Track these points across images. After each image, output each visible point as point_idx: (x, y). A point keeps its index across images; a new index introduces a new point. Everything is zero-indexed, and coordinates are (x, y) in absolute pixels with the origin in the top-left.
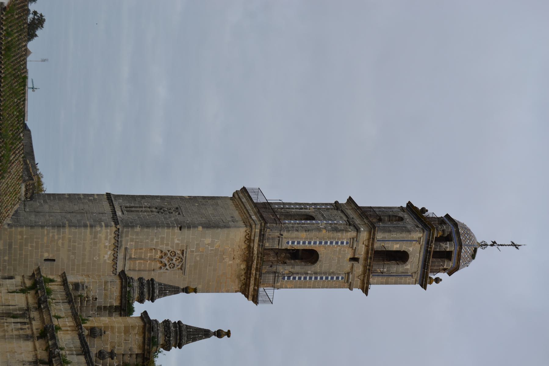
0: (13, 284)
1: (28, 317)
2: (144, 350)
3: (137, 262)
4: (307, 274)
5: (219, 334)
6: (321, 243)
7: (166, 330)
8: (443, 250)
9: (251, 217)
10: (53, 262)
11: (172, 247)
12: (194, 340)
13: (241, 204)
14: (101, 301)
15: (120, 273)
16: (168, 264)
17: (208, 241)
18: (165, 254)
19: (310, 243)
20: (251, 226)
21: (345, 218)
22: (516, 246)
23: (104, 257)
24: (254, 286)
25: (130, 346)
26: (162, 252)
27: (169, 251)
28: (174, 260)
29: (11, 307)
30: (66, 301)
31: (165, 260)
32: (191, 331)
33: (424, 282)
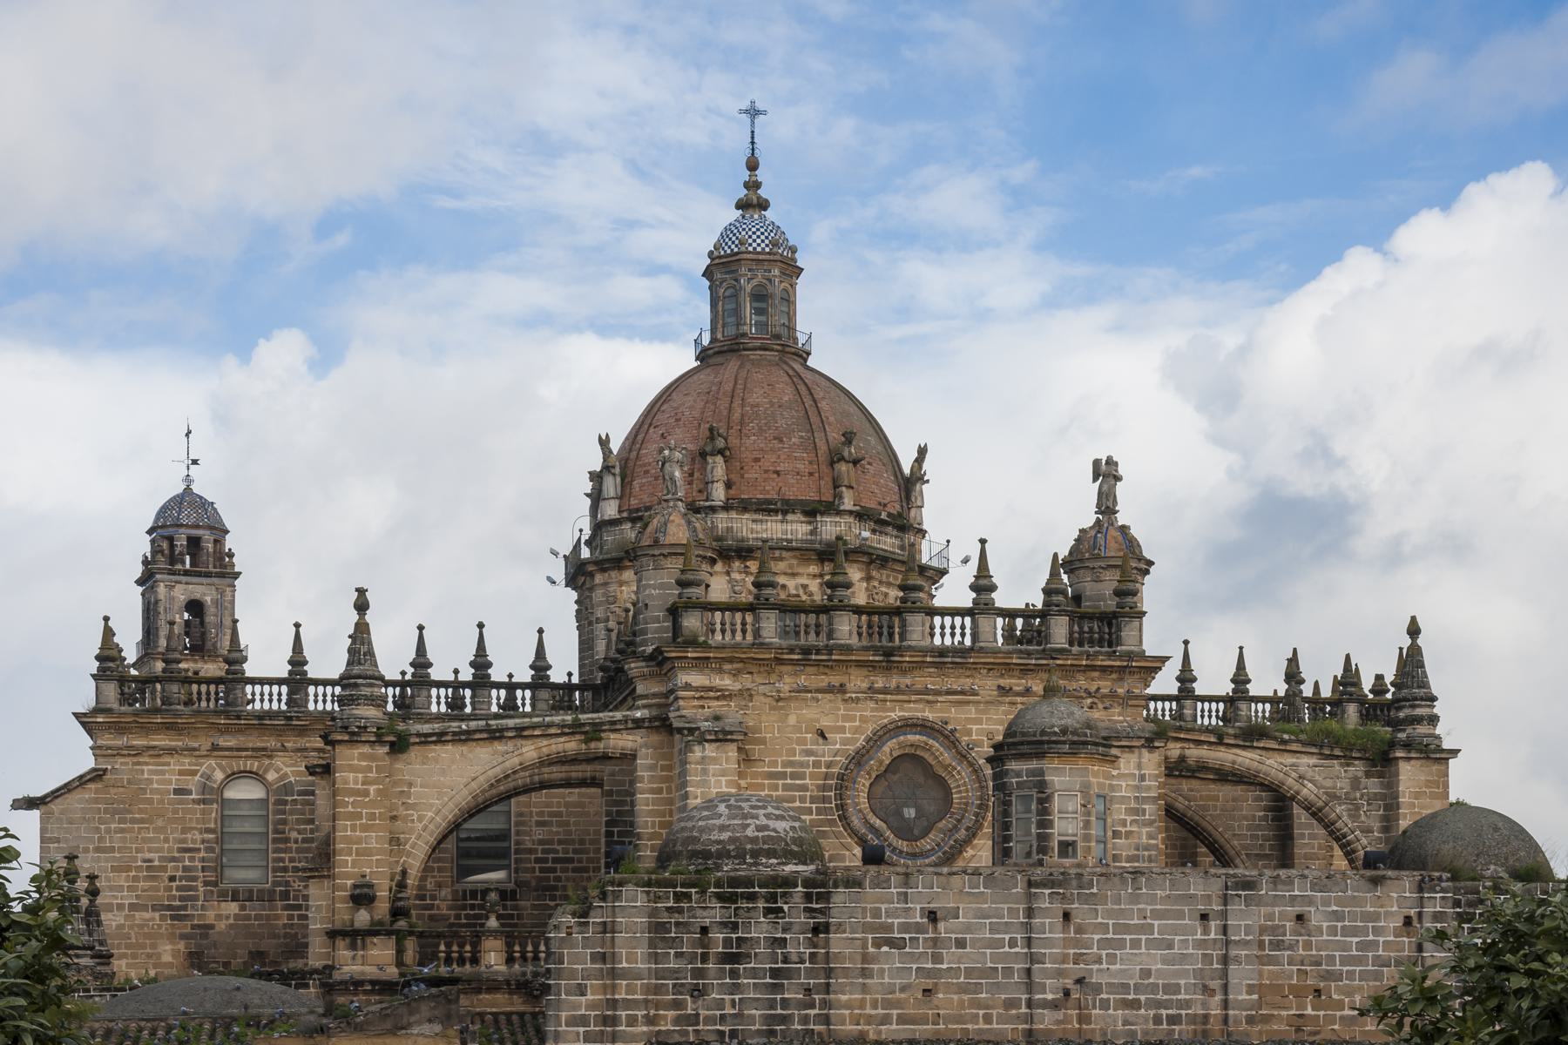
22: (188, 433)
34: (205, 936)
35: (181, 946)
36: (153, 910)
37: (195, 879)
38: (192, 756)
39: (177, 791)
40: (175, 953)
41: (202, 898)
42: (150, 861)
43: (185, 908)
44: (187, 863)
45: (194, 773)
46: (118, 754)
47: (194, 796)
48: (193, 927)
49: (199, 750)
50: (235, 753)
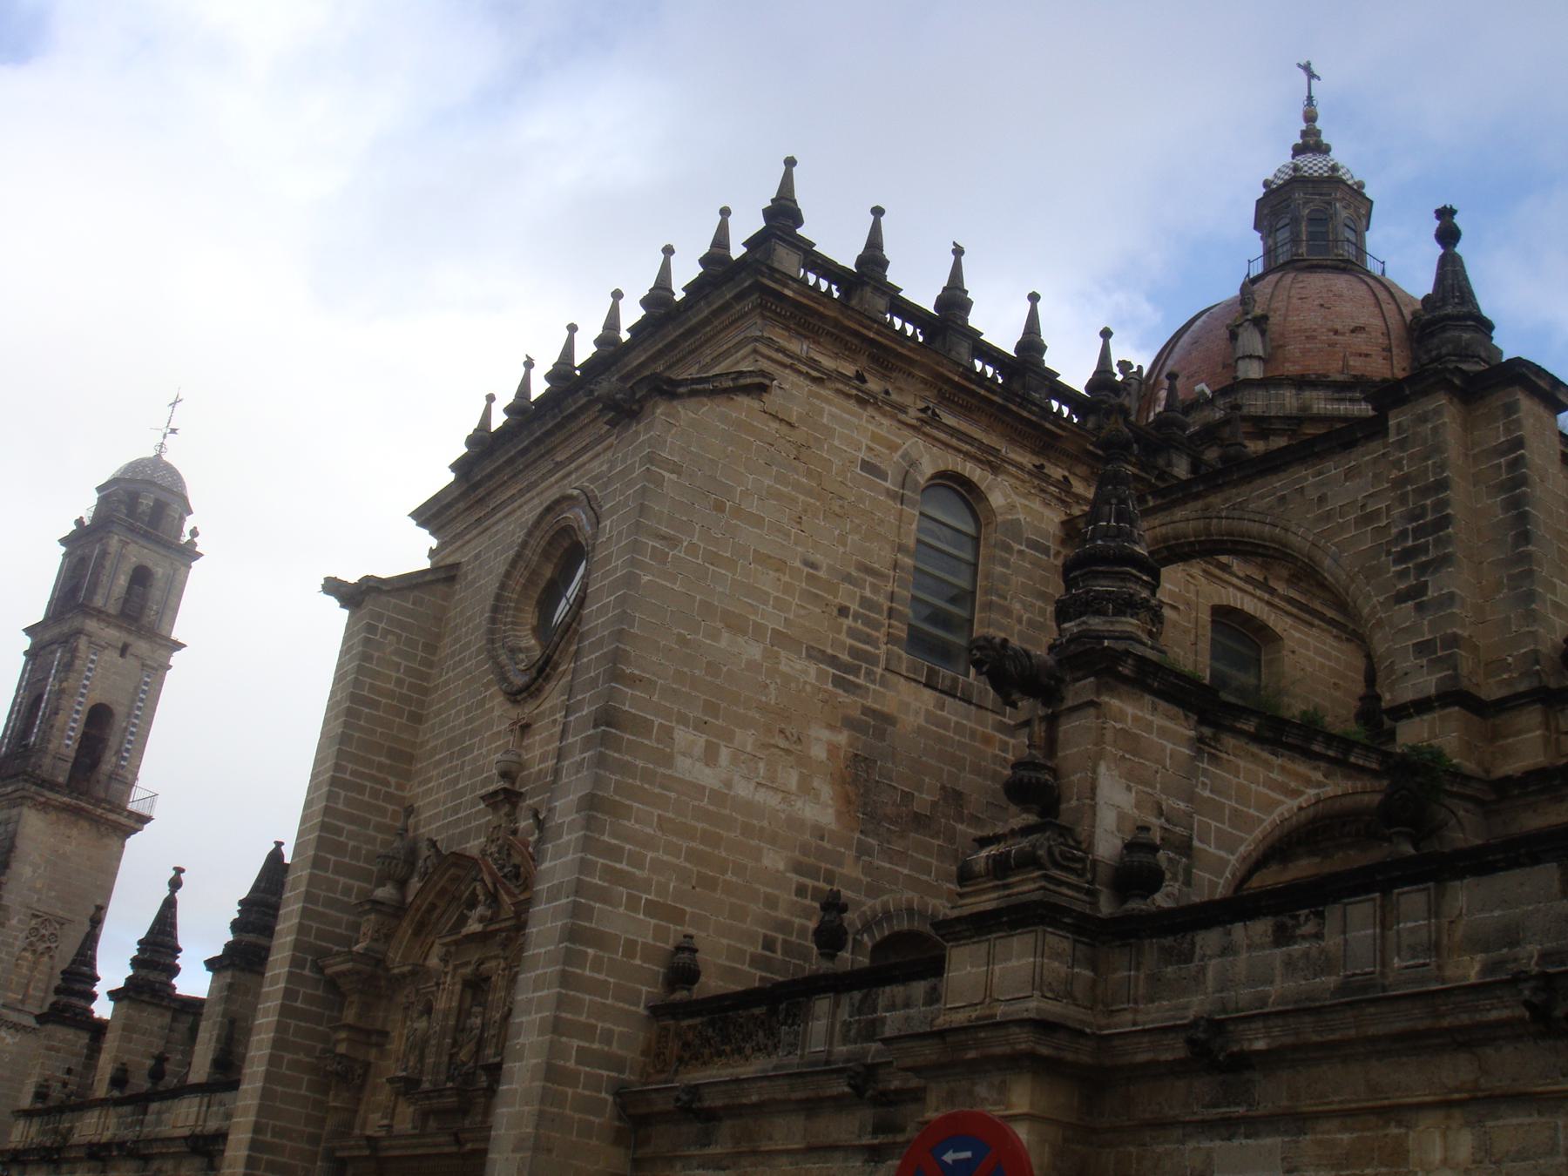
2: (166, 1008)
3: (31, 992)
4: (126, 729)
5: (175, 884)
6: (82, 695)
8: (149, 510)
11: (23, 930)
12: (174, 926)
16: (49, 945)
17: (27, 871)
18: (31, 944)
19: (77, 712)
20: (24, 797)
21: (55, 646)
23: (8, 1044)
26: (25, 949)
27: (27, 938)
28: (44, 932)
30: (58, 1118)
31: (41, 947)
33: (189, 554)
34: (881, 734)
35: (842, 738)
36: (809, 656)
37: (876, 626)
38: (893, 417)
39: (867, 466)
40: (833, 749)
41: (882, 664)
42: (813, 566)
43: (855, 671)
44: (868, 593)
45: (893, 447)
46: (791, 367)
47: (888, 484)
48: (867, 711)
49: (906, 413)
50: (954, 442)
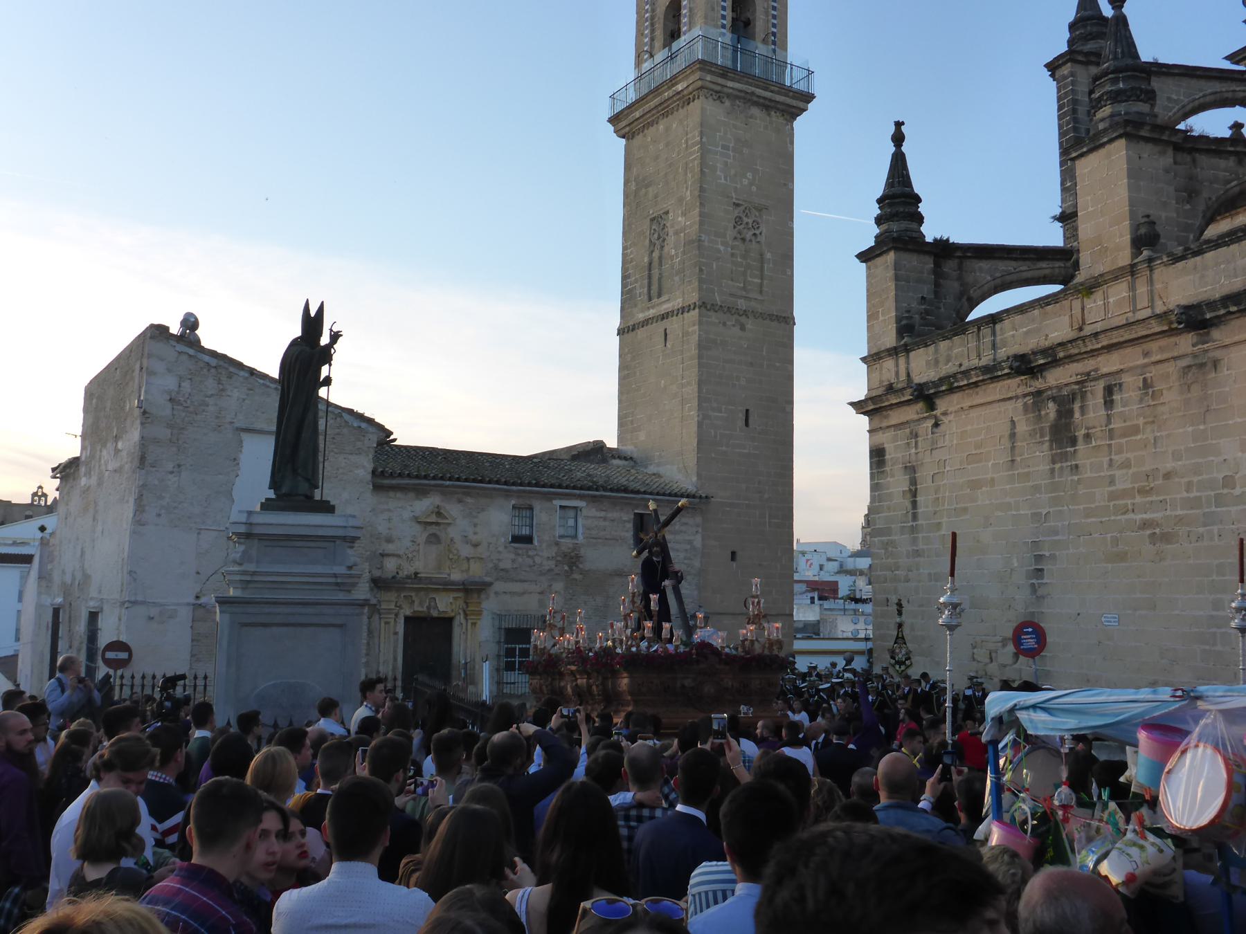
0: (908, 444)
1: (1077, 387)
2: (1167, 143)
7: (1124, 98)
9: (679, 93)
10: (750, 412)
13: (645, 118)
14: (927, 290)
15: (864, 259)
24: (788, 97)
25: (1161, 171)
27: (735, 227)
29: (1022, 428)
32: (1123, 52)
